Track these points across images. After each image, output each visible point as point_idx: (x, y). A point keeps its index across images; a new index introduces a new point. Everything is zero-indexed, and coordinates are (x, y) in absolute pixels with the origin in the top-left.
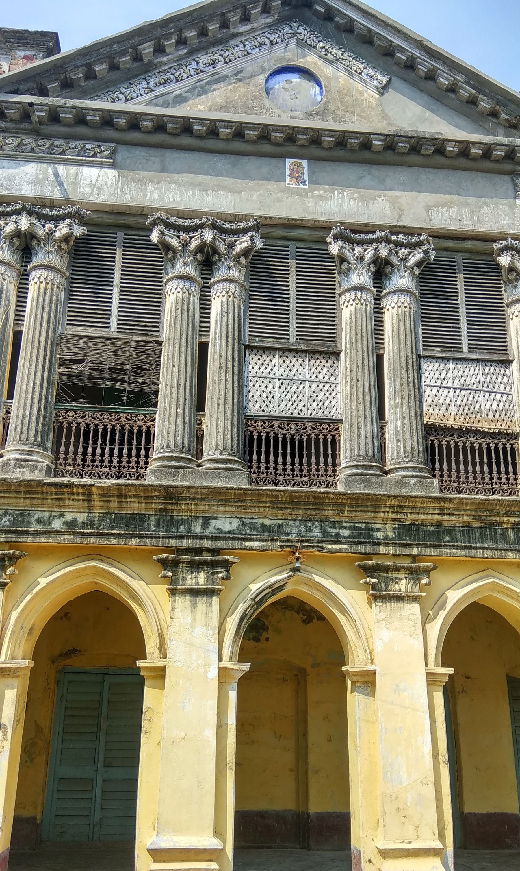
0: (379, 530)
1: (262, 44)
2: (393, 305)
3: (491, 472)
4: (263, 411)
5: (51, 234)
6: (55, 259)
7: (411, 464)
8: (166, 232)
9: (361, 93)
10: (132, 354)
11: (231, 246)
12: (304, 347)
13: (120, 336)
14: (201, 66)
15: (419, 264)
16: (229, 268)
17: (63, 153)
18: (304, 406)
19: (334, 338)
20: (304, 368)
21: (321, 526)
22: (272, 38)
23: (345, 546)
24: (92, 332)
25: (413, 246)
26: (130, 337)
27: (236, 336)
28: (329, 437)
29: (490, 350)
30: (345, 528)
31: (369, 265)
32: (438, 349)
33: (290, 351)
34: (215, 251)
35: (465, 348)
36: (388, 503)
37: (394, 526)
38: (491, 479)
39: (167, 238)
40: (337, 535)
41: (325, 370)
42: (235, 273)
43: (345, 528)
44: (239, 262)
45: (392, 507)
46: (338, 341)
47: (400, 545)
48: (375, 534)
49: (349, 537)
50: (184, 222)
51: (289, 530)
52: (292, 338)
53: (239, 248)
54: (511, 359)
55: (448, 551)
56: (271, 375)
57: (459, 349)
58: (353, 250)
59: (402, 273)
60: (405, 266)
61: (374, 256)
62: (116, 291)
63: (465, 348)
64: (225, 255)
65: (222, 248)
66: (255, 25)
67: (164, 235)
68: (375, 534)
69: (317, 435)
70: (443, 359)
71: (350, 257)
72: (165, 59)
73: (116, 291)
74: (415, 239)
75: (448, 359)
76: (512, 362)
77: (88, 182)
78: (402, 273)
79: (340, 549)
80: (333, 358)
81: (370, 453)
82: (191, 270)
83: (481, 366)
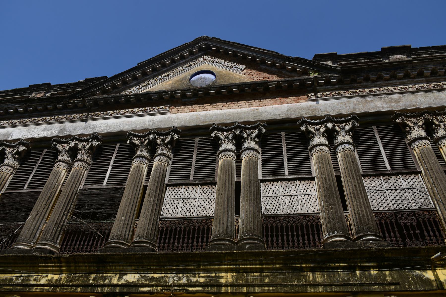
0: (222, 277)
1: (190, 66)
2: (244, 156)
3: (303, 240)
4: (171, 215)
5: (84, 147)
6: (85, 157)
7: (248, 237)
8: (134, 138)
9: (233, 75)
10: (111, 195)
11: (163, 140)
12: (197, 182)
13: (107, 187)
14: (163, 77)
15: (257, 136)
16: (162, 150)
17: (98, 116)
18: (194, 211)
19: (213, 177)
20: (197, 192)
21: (187, 276)
22: (194, 63)
23: (200, 289)
24: (95, 187)
25: (254, 128)
26: (111, 187)
27: (160, 180)
28: (206, 227)
29: (301, 173)
30: (202, 277)
31: (232, 140)
32: (271, 176)
33: (190, 185)
34: (157, 144)
35: (286, 172)
36: (226, 259)
37: (233, 274)
38: (304, 244)
39: (134, 141)
40: (197, 281)
41: (208, 192)
42: (165, 152)
43: (202, 277)
44: (167, 147)
45: (229, 261)
46: (215, 177)
47: (235, 286)
48: (220, 280)
49: (204, 282)
50: (143, 133)
51: (167, 280)
52: (191, 178)
53: (167, 141)
54: (313, 176)
55: (267, 288)
56: (179, 197)
57: (284, 175)
58: (224, 134)
59: (249, 141)
60: (251, 138)
61: (234, 135)
62: (110, 168)
63: (286, 172)
64: (161, 144)
65: (159, 141)
66: (187, 60)
67: (133, 140)
68: (220, 280)
69: (199, 227)
70: (274, 180)
71: (222, 137)
72: (147, 77)
73: (110, 168)
74: (255, 125)
75: (277, 180)
76: (314, 177)
77: (105, 125)
78: (249, 141)
79: (197, 290)
80: (213, 186)
81: (225, 232)
82: (144, 153)
83: (298, 182)
